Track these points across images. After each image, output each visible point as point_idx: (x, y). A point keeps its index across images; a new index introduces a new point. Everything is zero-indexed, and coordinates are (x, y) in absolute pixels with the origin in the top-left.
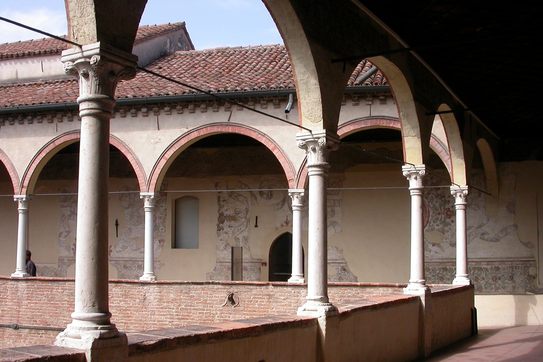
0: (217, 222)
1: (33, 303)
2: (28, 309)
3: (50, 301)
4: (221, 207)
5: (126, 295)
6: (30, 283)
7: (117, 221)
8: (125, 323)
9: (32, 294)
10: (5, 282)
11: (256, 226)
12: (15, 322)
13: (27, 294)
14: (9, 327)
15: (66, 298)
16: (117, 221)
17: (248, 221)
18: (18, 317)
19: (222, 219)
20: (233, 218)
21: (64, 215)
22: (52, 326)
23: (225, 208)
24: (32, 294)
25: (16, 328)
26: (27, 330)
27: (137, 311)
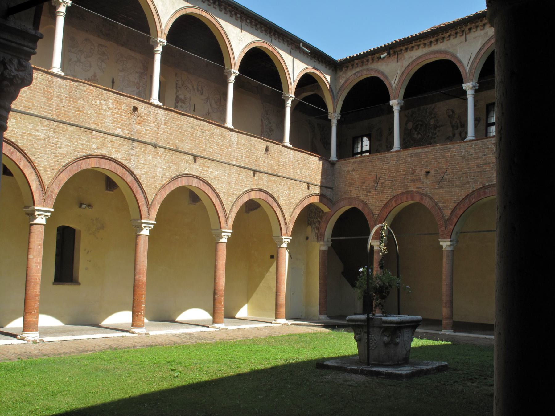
0: (174, 101)
1: (168, 129)
2: (164, 132)
3: (179, 129)
4: (177, 91)
5: (222, 135)
6: (167, 112)
7: (113, 79)
8: (221, 155)
9: (168, 121)
10: (149, 106)
11: (194, 111)
12: (154, 141)
13: (165, 120)
14: (151, 144)
15: (189, 130)
16: (113, 79)
17: (190, 106)
18: (157, 138)
19: (177, 100)
20: (183, 102)
21: (70, 60)
22: (179, 149)
23: (180, 93)
24: (168, 121)
25: (155, 146)
26: (163, 149)
27: (227, 148)
